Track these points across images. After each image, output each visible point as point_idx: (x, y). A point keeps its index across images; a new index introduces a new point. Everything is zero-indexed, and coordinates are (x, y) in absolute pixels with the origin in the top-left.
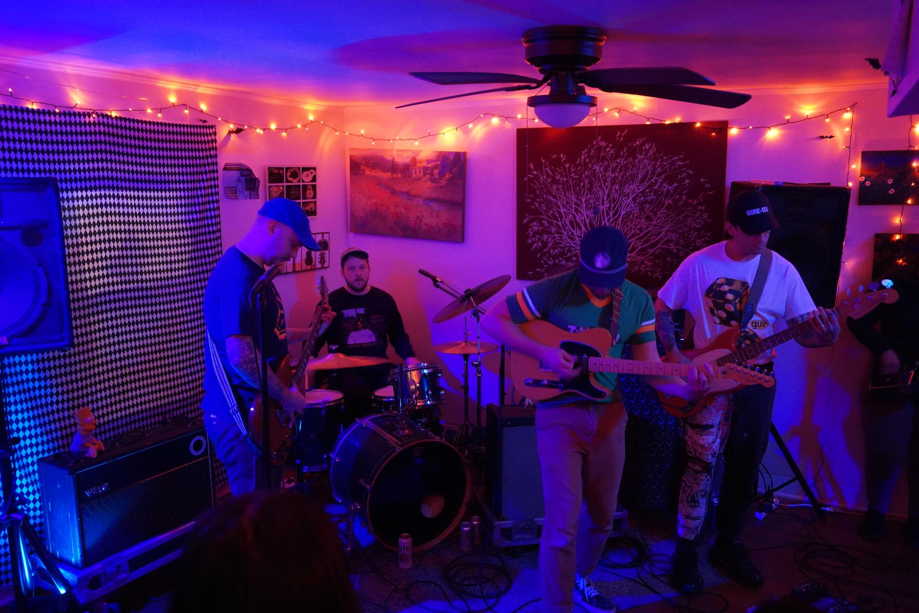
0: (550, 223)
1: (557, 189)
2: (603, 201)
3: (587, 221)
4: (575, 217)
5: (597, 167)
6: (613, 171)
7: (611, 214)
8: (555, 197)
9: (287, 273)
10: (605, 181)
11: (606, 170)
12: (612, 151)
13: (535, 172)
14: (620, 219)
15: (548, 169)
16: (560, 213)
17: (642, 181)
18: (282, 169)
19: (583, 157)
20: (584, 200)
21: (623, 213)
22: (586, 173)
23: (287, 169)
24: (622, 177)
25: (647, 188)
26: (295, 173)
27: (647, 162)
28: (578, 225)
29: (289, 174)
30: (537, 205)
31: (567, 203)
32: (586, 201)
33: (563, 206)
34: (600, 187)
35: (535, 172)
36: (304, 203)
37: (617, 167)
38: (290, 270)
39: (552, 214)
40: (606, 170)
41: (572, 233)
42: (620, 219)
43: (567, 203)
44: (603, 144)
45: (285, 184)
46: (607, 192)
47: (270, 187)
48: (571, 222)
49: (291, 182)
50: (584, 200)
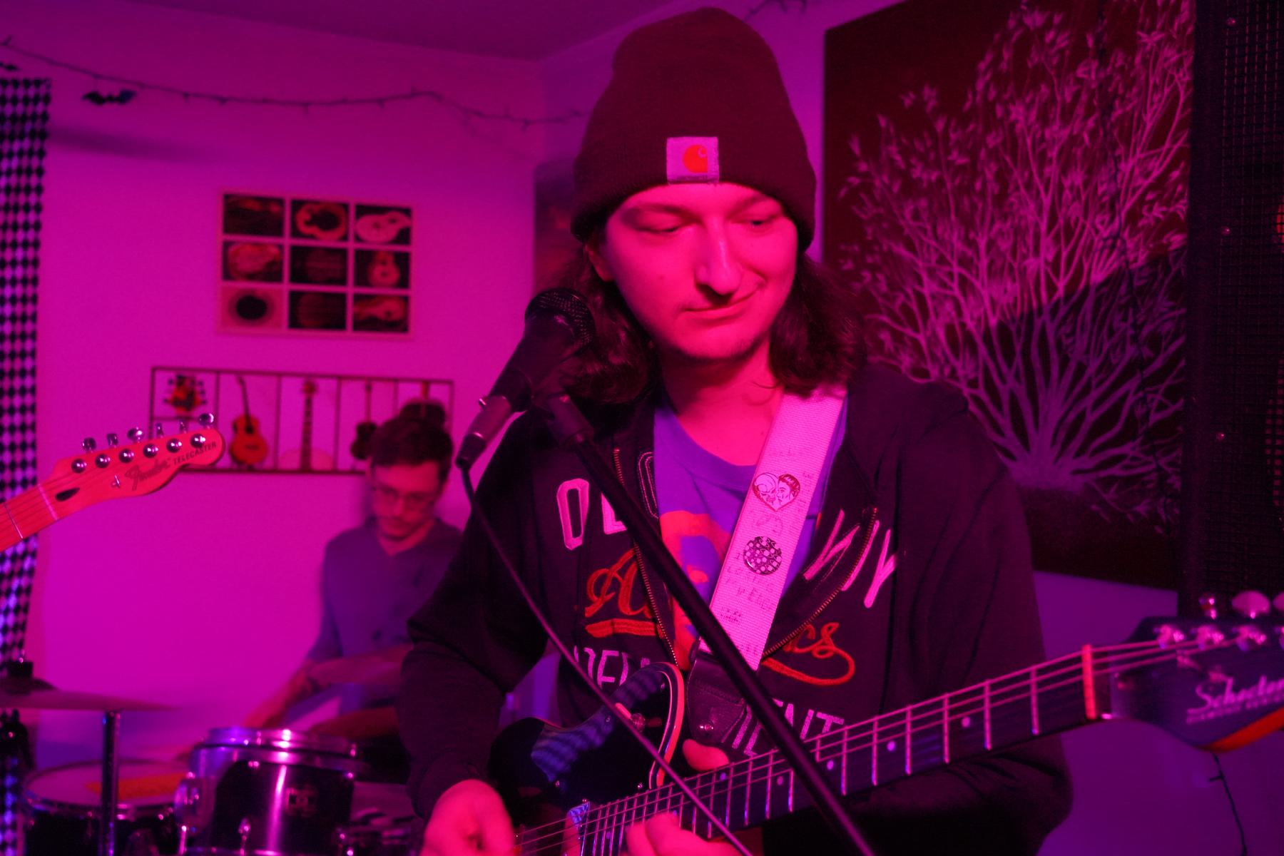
0: (897, 337)
1: (916, 216)
2: (1037, 236)
3: (993, 322)
4: (960, 314)
5: (1017, 112)
6: (1067, 115)
7: (1061, 285)
8: (910, 246)
9: (275, 471)
10: (1043, 160)
11: (1044, 120)
12: (1063, 41)
13: (863, 167)
14: (1088, 304)
15: (893, 149)
16: (920, 298)
17: (1157, 140)
18: (280, 202)
19: (980, 86)
20: (982, 244)
21: (1098, 277)
22: (992, 140)
23: (297, 205)
24: (1093, 134)
25: (1173, 166)
26: (327, 218)
27: (1171, 54)
28: (968, 337)
29: (303, 216)
30: (867, 275)
31: (942, 261)
32: (991, 244)
33: (931, 272)
34: (1029, 185)
35: (863, 167)
36: (358, 298)
37: (1076, 96)
38: (293, 462)
39: (904, 307)
40: (1044, 120)
41: (953, 371)
42: (1088, 304)
43: (942, 261)
44: (1035, 19)
45: (287, 241)
46: (1046, 201)
47: (226, 245)
48: (950, 329)
49: (312, 237)
50: (982, 244)
